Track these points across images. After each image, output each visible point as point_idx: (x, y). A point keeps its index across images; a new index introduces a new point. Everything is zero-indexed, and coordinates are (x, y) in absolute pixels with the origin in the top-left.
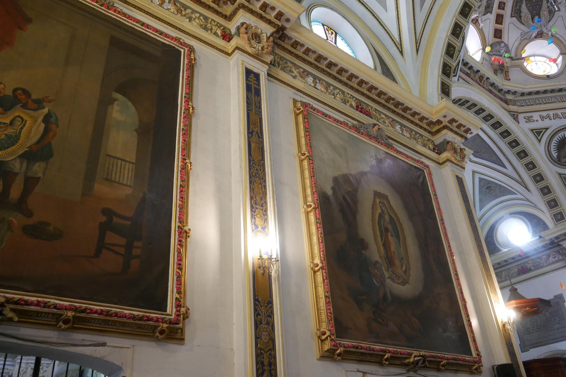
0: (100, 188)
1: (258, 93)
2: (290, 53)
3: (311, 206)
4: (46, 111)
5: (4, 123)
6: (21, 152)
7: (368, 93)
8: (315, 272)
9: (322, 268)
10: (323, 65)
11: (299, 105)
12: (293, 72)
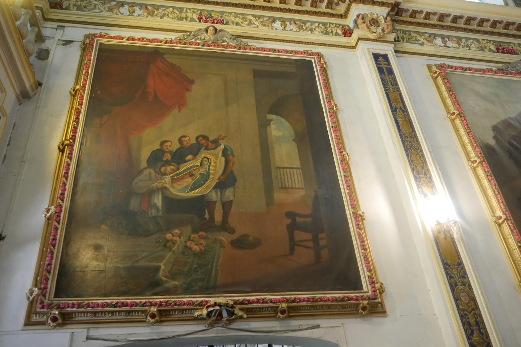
0: (279, 196)
1: (390, 72)
2: (411, 23)
3: (476, 161)
4: (222, 147)
5: (197, 166)
6: (214, 184)
7: (505, 31)
8: (499, 225)
9: (507, 219)
10: (448, 22)
11: (434, 69)
12: (419, 40)
